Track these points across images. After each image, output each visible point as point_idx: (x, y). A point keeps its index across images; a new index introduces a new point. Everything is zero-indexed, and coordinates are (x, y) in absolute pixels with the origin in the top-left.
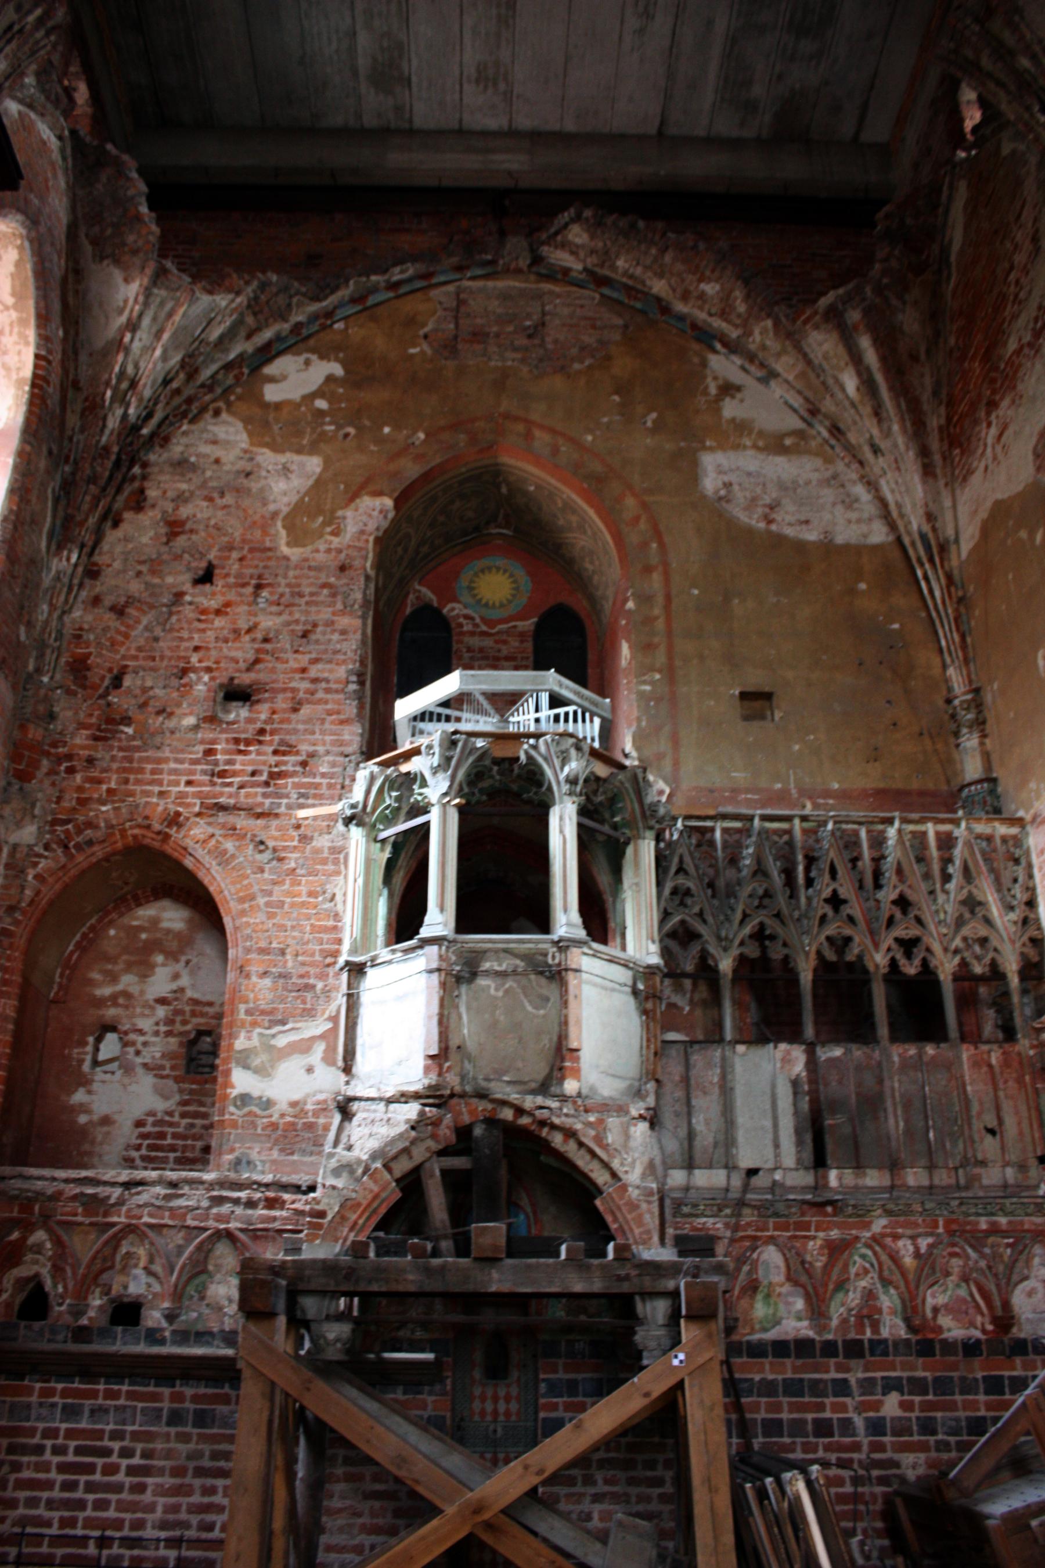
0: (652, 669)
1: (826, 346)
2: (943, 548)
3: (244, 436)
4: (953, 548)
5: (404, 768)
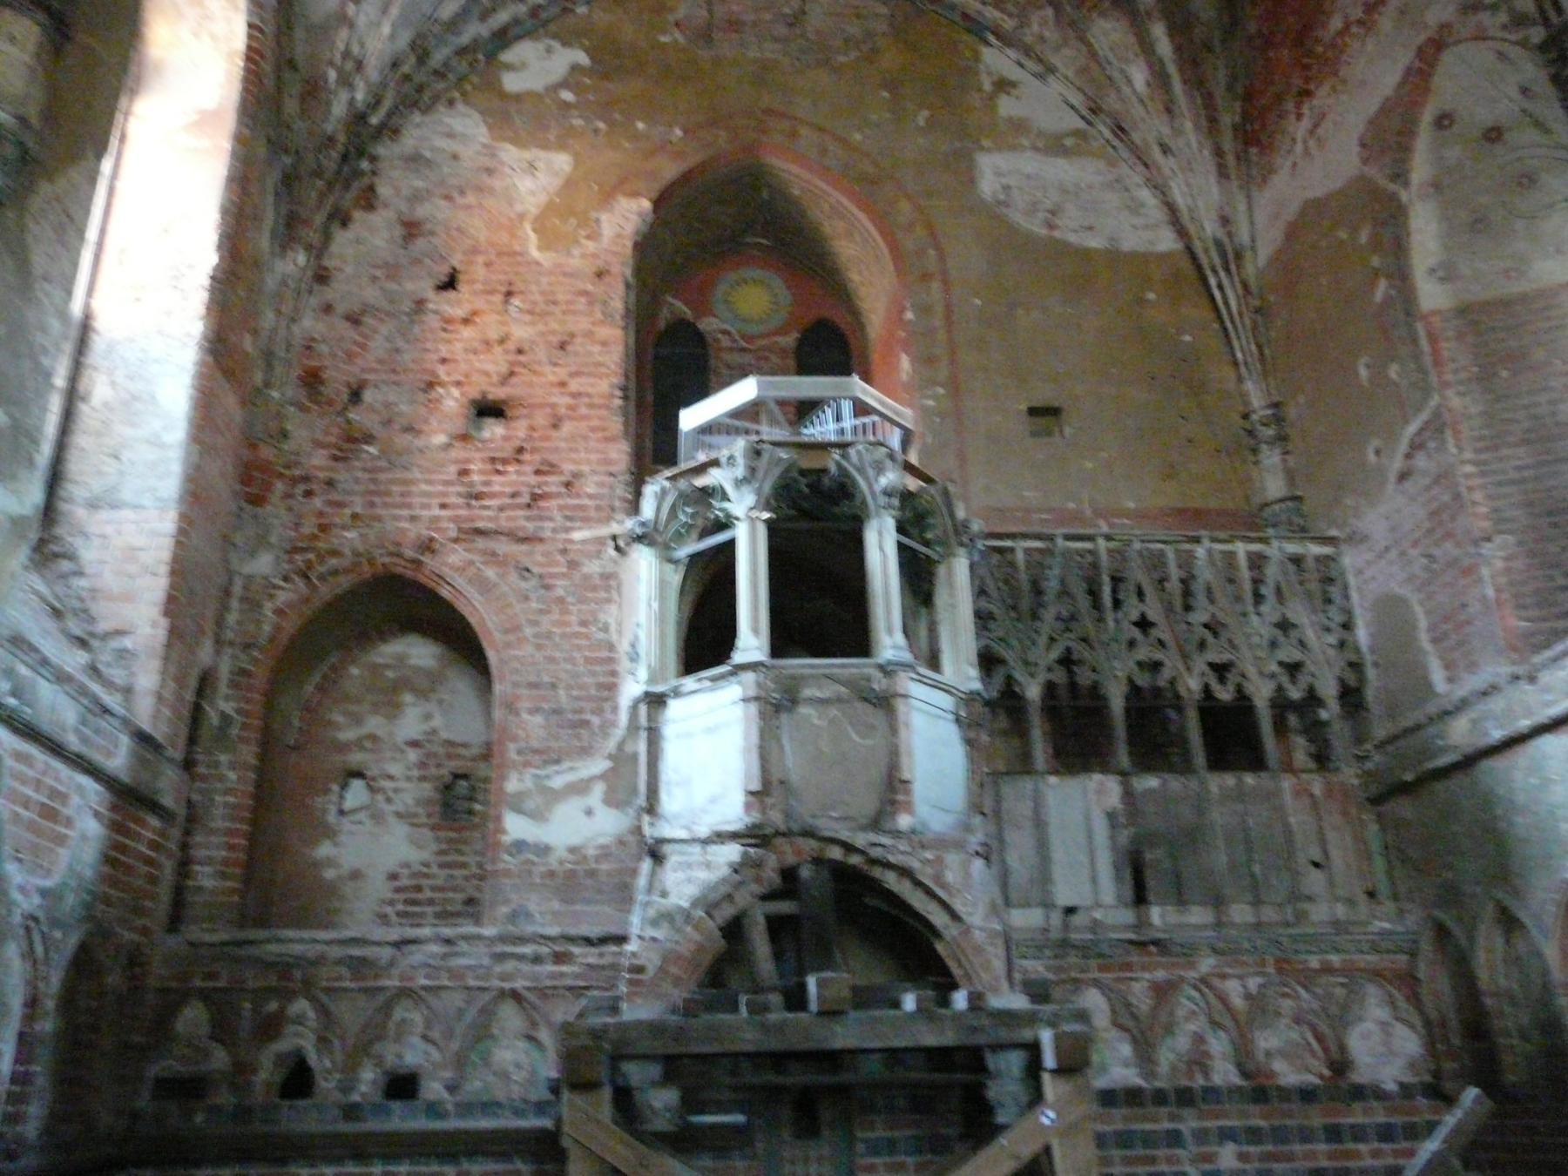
0: (936, 383)
1: (1116, 37)
2: (1239, 256)
3: (483, 130)
4: (1248, 254)
5: (700, 482)
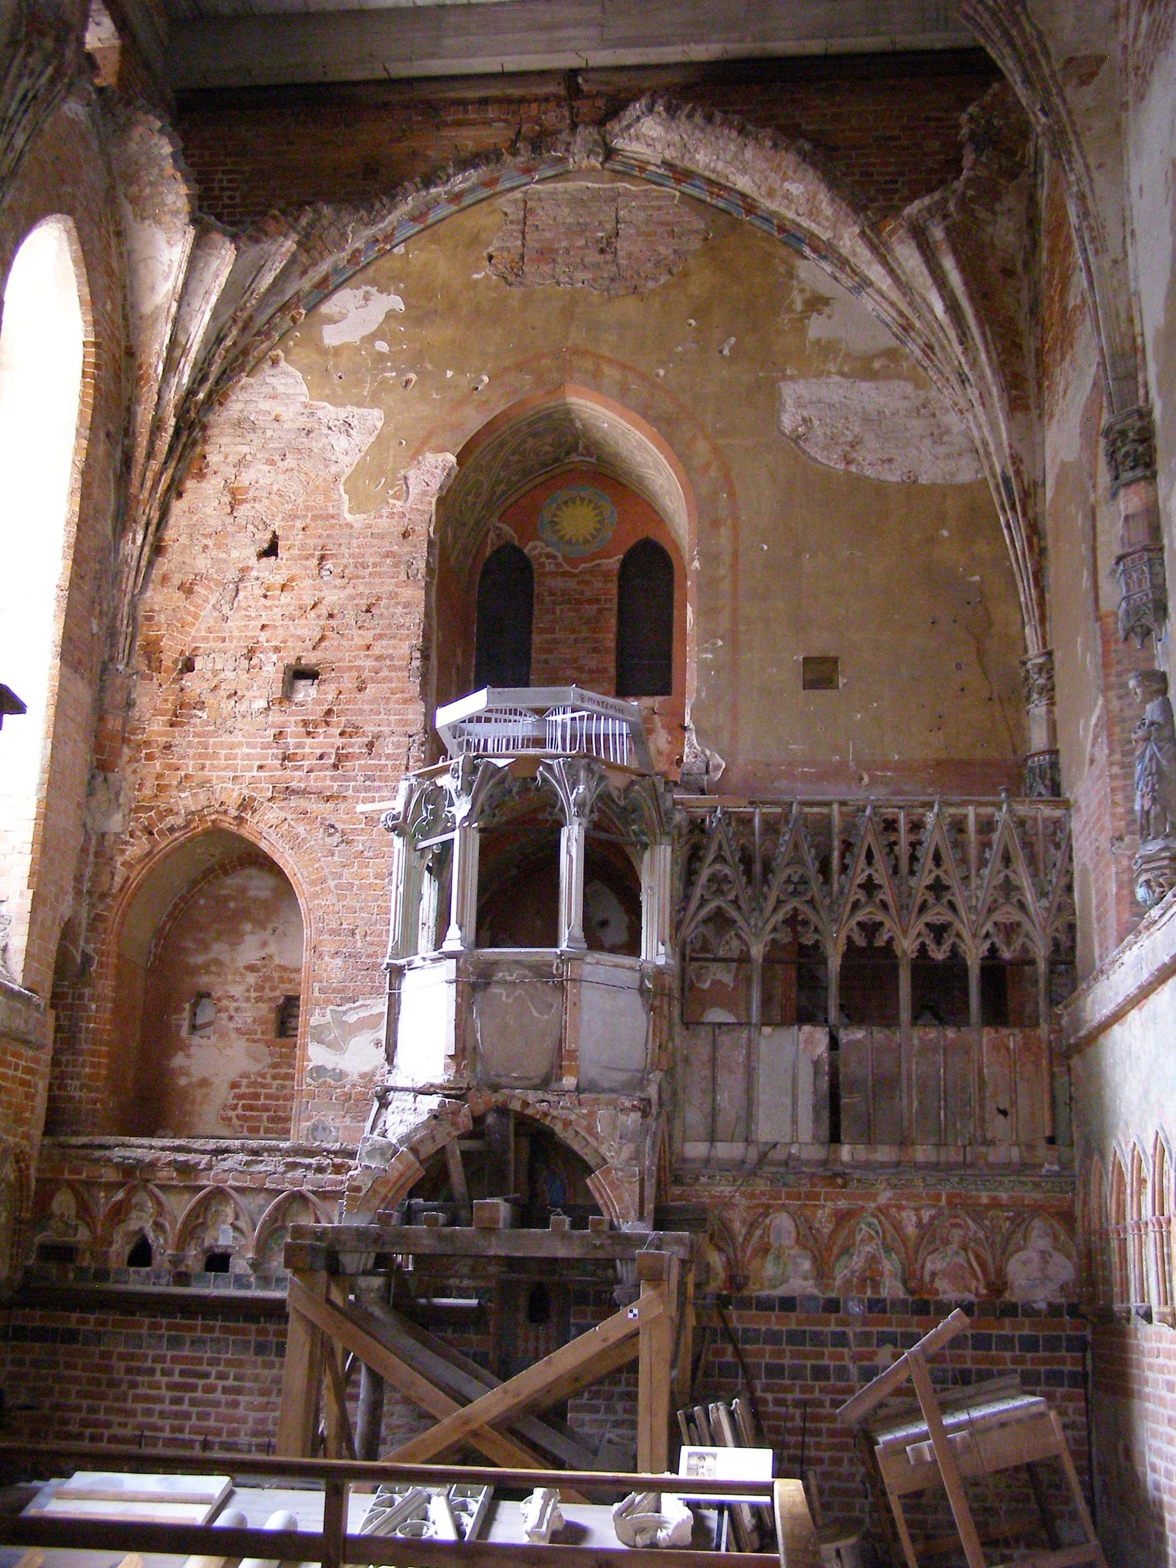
0: (715, 635)
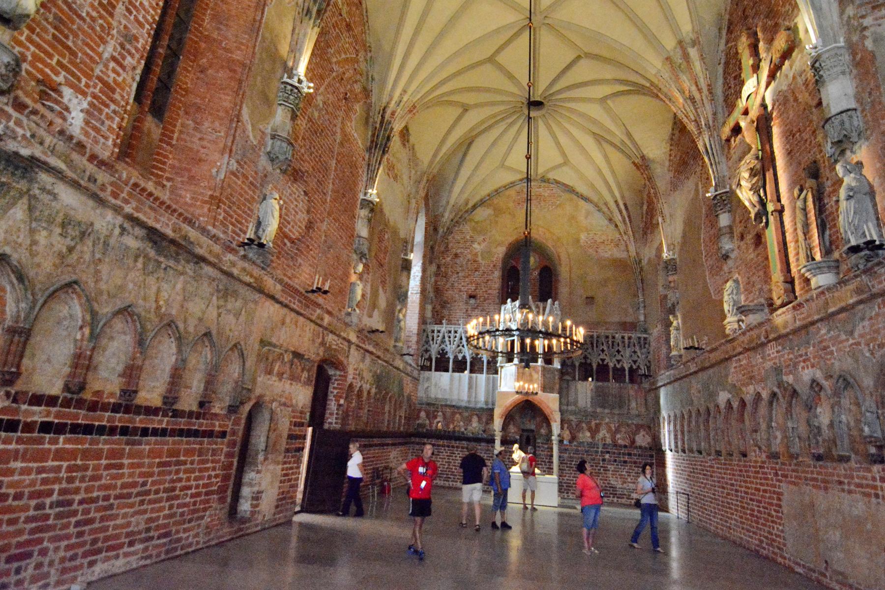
2: (640, 261)
